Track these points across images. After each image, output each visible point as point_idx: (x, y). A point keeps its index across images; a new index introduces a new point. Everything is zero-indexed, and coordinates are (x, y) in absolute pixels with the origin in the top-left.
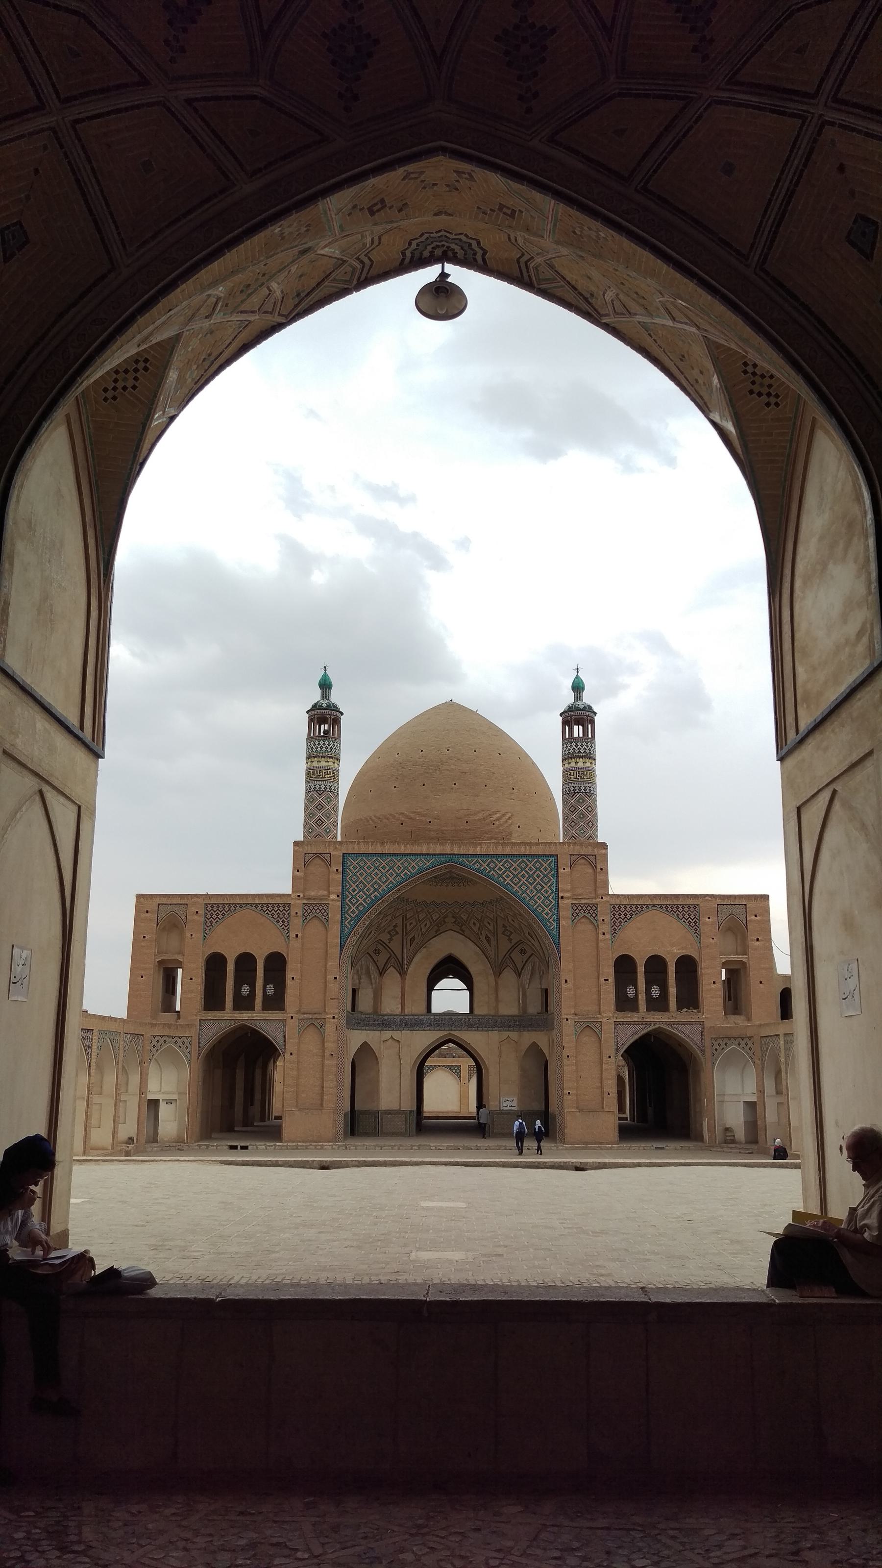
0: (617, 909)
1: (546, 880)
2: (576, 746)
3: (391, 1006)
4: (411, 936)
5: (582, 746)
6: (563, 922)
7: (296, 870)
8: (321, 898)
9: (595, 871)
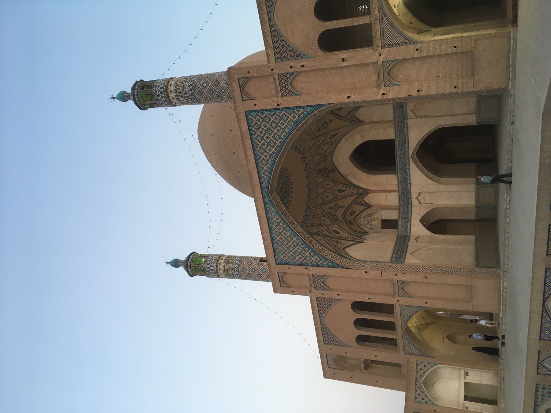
0: (279, 55)
1: (267, 119)
2: (161, 100)
3: (393, 199)
4: (337, 193)
5: (159, 95)
6: (298, 104)
7: (293, 293)
8: (310, 279)
9: (252, 78)
